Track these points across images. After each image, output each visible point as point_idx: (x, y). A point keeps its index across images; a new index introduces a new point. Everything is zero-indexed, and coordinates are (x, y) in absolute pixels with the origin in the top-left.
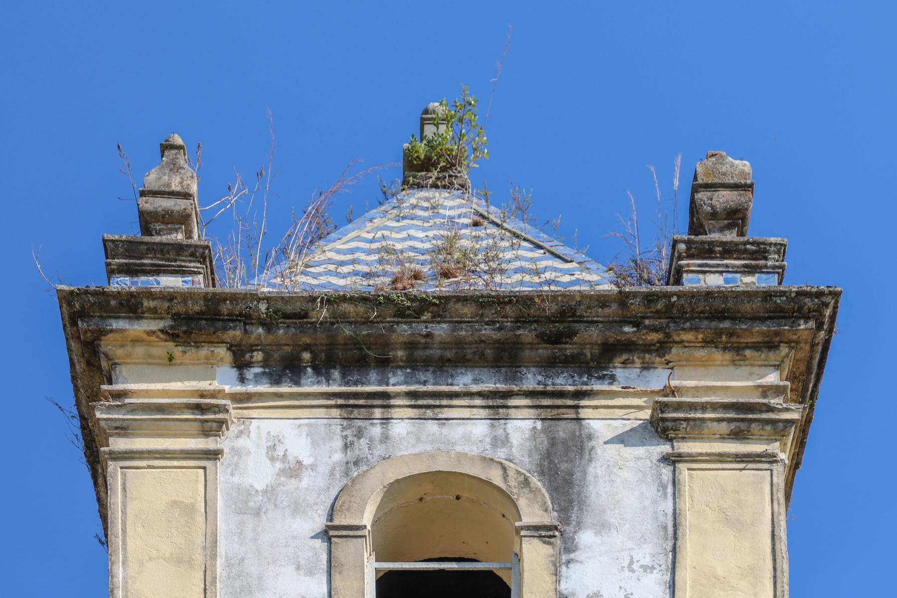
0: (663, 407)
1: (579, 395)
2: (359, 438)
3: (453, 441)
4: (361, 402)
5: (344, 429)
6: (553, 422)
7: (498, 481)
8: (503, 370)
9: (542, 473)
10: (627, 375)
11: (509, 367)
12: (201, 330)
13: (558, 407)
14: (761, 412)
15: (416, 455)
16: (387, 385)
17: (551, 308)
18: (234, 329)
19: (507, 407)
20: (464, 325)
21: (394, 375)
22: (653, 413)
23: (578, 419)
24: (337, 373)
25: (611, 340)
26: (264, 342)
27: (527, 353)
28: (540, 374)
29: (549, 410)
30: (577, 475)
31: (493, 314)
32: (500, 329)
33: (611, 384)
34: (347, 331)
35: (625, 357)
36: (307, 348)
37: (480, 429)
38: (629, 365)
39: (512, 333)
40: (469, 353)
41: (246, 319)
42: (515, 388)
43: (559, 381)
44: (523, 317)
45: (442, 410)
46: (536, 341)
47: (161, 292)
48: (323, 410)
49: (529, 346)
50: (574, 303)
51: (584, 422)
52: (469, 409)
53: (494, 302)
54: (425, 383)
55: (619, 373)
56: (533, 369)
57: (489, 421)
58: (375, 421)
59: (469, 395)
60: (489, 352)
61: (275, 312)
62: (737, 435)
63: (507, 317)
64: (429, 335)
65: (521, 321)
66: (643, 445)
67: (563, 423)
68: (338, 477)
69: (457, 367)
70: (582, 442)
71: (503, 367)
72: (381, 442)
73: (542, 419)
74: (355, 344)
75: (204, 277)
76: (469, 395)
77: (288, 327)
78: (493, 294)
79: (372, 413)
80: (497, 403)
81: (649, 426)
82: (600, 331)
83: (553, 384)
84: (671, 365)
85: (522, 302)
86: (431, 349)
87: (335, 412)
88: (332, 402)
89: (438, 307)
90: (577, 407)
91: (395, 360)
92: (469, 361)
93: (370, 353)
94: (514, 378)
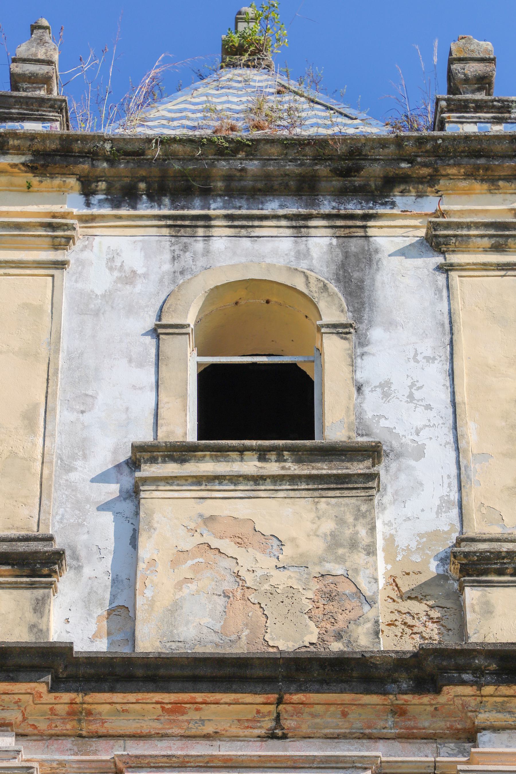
0: (436, 226)
2: (185, 252)
4: (187, 223)
6: (346, 239)
8: (304, 198)
10: (405, 201)
11: (309, 195)
12: (56, 164)
13: (350, 227)
15: (232, 266)
16: (209, 209)
17: (341, 149)
18: (83, 163)
19: (308, 227)
20: (272, 162)
21: (215, 202)
22: (427, 231)
23: (366, 237)
24: (167, 200)
25: (391, 174)
26: (108, 175)
27: (323, 185)
28: (334, 201)
29: (342, 230)
31: (295, 153)
32: (301, 165)
33: (392, 208)
34: (177, 166)
35: (402, 187)
36: (143, 179)
38: (406, 194)
39: (311, 168)
40: (276, 184)
41: (94, 155)
42: (314, 212)
43: (350, 206)
44: (319, 156)
45: (254, 229)
46: (330, 175)
47: (24, 133)
49: (325, 179)
50: (360, 145)
51: (371, 239)
52: (276, 229)
53: (296, 144)
54: (240, 208)
55: (398, 200)
56: (329, 197)
57: (293, 238)
61: (118, 151)
63: (306, 156)
64: (243, 170)
65: (318, 159)
66: (421, 256)
68: (167, 284)
69: (266, 195)
70: (370, 255)
71: (305, 195)
72: (203, 255)
73: (337, 237)
74: (182, 177)
75: (61, 124)
77: (128, 162)
78: (295, 137)
79: (196, 232)
80: (299, 224)
81: (425, 242)
82: (382, 166)
83: (345, 209)
84: (440, 193)
85: (320, 143)
86: (245, 181)
88: (163, 223)
89: (250, 148)
90: (365, 227)
92: (276, 190)
94: (313, 204)
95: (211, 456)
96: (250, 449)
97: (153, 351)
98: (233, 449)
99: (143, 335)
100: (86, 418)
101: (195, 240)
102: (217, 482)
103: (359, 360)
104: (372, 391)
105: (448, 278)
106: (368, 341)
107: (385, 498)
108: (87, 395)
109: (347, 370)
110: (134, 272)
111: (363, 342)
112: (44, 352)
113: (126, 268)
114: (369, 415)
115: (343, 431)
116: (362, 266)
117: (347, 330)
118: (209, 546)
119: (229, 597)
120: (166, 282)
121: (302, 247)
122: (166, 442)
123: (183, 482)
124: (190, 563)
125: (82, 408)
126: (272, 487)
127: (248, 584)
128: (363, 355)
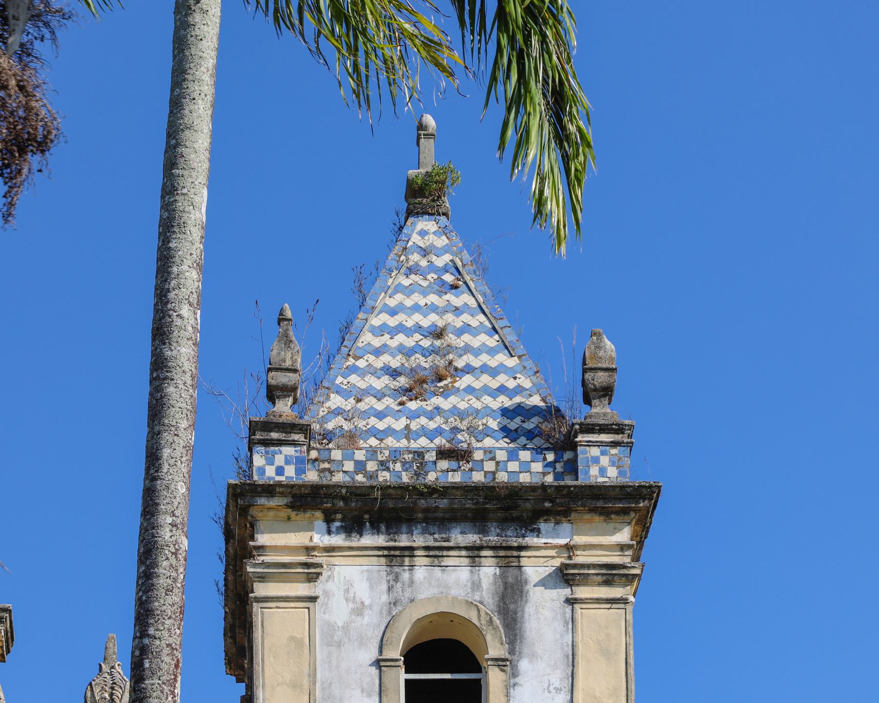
5: (388, 574)
9: (499, 613)
14: (620, 569)
23: (520, 567)
27: (491, 515)
48: (376, 558)
62: (608, 582)
66: (555, 587)
67: (511, 569)
88: (380, 553)
90: (519, 557)
110: (362, 603)
111: (515, 675)
112: (306, 683)
113: (357, 599)
117: (504, 663)
120: (385, 612)
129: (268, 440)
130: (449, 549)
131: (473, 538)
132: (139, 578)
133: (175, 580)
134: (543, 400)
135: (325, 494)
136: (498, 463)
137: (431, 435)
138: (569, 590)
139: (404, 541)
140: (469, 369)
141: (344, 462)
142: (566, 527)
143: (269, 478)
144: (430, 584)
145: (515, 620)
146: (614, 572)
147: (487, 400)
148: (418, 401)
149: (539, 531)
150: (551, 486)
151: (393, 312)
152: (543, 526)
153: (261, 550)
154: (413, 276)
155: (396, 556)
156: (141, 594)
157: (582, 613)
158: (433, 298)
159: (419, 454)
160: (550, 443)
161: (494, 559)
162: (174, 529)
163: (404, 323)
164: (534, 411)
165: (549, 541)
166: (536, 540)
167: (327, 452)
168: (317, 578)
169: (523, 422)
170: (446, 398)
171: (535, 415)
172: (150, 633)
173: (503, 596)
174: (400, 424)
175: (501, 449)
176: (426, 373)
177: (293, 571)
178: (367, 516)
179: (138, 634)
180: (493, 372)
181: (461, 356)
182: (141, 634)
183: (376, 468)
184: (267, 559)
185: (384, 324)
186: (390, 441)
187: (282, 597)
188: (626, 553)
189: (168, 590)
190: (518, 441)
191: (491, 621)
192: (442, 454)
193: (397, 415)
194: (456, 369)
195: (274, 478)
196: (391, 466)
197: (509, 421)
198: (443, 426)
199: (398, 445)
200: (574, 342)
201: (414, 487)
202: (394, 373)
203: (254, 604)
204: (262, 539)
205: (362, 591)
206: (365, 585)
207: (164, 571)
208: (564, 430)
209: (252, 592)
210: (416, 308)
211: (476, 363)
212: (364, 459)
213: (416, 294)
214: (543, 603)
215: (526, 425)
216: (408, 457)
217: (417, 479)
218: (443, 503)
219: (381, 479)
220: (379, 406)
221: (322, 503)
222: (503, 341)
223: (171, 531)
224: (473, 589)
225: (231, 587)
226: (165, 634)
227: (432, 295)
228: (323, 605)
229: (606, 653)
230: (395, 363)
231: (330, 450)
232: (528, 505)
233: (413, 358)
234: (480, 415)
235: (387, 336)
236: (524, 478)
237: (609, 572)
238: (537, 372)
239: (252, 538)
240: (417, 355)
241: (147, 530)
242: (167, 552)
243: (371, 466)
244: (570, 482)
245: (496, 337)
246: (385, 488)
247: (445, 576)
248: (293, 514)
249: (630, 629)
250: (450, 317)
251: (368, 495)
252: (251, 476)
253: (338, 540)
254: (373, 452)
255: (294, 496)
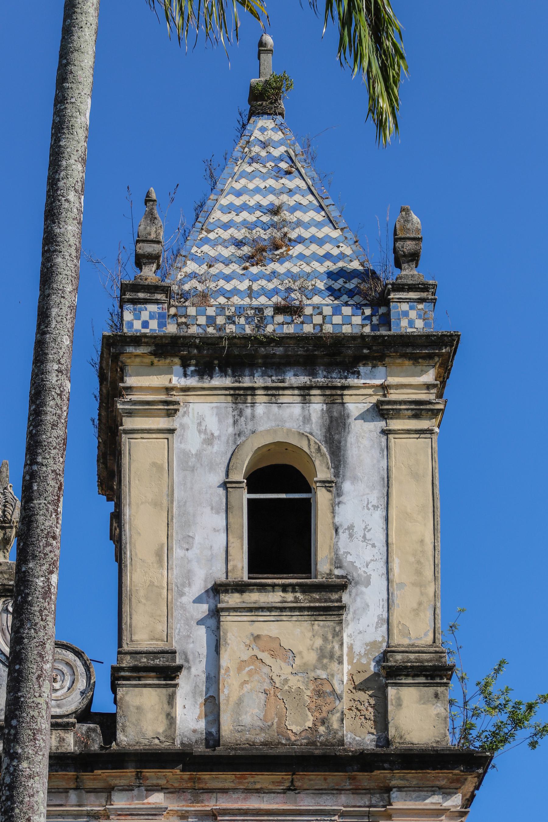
1: (344, 388)
2: (241, 417)
3: (285, 419)
4: (241, 392)
7: (306, 449)
8: (308, 368)
9: (326, 442)
21: (257, 372)
30: (343, 443)
37: (297, 410)
48: (224, 397)
52: (292, 396)
56: (322, 367)
57: (301, 404)
58: (249, 405)
59: (292, 388)
60: (301, 360)
70: (345, 420)
76: (292, 388)
87: (229, 398)
90: (342, 395)
91: (258, 363)
93: (246, 361)
95: (257, 589)
96: (278, 585)
97: (224, 500)
98: (269, 585)
99: (218, 487)
100: (190, 554)
101: (247, 406)
102: (261, 610)
103: (337, 507)
104: (343, 532)
105: (387, 439)
106: (342, 492)
107: (348, 616)
108: (189, 536)
109: (330, 515)
110: (212, 434)
114: (341, 552)
115: (328, 565)
116: (340, 429)
117: (330, 485)
118: (257, 657)
119: (267, 694)
121: (307, 412)
122: (233, 582)
123: (242, 610)
124: (247, 669)
125: (187, 547)
126: (289, 614)
127: (277, 686)
128: (339, 503)
129: (136, 299)
130: (284, 388)
131: (303, 380)
132: (30, 415)
133: (60, 417)
134: (362, 264)
135: (182, 344)
136: (324, 317)
137: (269, 294)
138: (384, 422)
139: (247, 382)
140: (300, 240)
141: (198, 317)
142: (381, 369)
143: (137, 331)
144: (268, 418)
145: (339, 448)
146: (421, 407)
147: (315, 265)
148: (259, 267)
149: (358, 373)
150: (368, 336)
151: (238, 194)
152: (362, 369)
153: (129, 390)
154: (254, 165)
155: (240, 396)
156: (31, 428)
157: (395, 442)
158: (271, 182)
159: (260, 310)
160: (368, 300)
161: (321, 397)
162: (60, 374)
163: (247, 202)
164: (354, 274)
165: (368, 381)
166: (356, 381)
167: (184, 309)
168: (175, 413)
169: (345, 282)
170: (281, 264)
171: (354, 277)
172: (38, 461)
173: (329, 428)
174: (243, 286)
175: (327, 305)
176: (265, 243)
177: (155, 407)
178: (216, 362)
179: (28, 462)
180: (320, 242)
181: (294, 229)
182: (31, 461)
183: (224, 322)
184: (135, 397)
185: (231, 203)
186: (236, 300)
187: (146, 430)
188: (432, 391)
189: (53, 425)
190: (341, 299)
191: (319, 450)
192: (279, 310)
193: (241, 278)
194: (290, 240)
195: (140, 330)
196: (237, 320)
197: (333, 282)
198: (280, 287)
199: (242, 303)
200: (388, 219)
201: (255, 338)
202: (239, 244)
203: (123, 435)
204: (131, 381)
205: (212, 424)
206: (215, 419)
207: (51, 409)
208: (379, 289)
209: (122, 425)
210: (257, 190)
211: (306, 234)
212: (214, 314)
213: (257, 179)
214: (363, 434)
215: (347, 286)
216: (251, 312)
217: (258, 331)
218: (279, 351)
219: (228, 331)
220: (227, 271)
221: (180, 351)
222: (328, 217)
223: (57, 376)
224: (304, 423)
225: (104, 421)
226: (51, 461)
227: (270, 180)
228: (179, 436)
229: (416, 476)
230: (239, 235)
231: (186, 307)
232: (350, 352)
233: (254, 231)
234: (310, 277)
235: (234, 213)
236: (347, 329)
237: (418, 407)
238: (356, 242)
239: (122, 380)
240: (258, 229)
241: (37, 375)
242: (53, 393)
243: (220, 320)
244: (384, 333)
245: (323, 213)
246: (231, 338)
247: (280, 411)
248: (156, 360)
249: (436, 455)
250: (284, 198)
251: (218, 344)
252: (121, 329)
253: (192, 382)
254: (221, 308)
255: (156, 345)
